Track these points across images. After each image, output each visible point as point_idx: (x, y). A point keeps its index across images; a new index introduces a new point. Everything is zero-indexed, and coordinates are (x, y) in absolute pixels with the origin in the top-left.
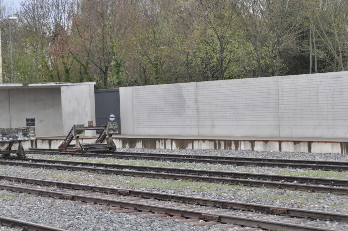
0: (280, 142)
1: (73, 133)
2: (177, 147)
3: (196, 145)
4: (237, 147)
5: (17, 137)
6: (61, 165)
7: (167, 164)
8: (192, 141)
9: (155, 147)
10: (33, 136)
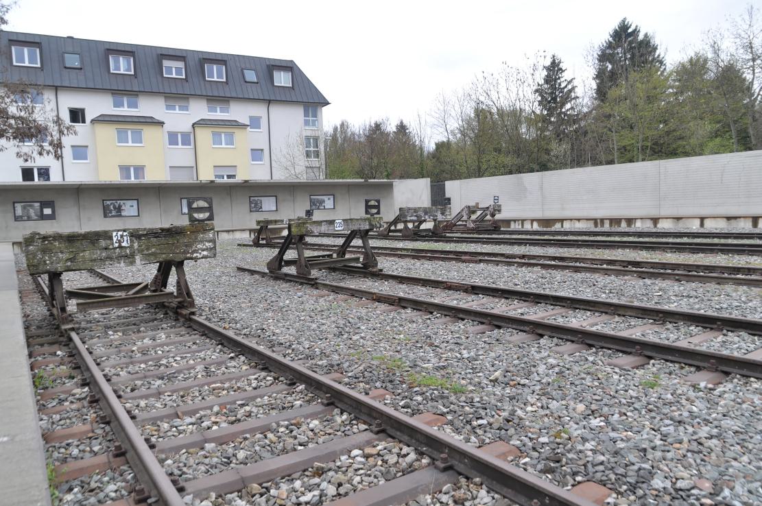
0: (702, 219)
1: (464, 214)
2: (539, 226)
5: (437, 216)
8: (562, 221)
10: (450, 215)
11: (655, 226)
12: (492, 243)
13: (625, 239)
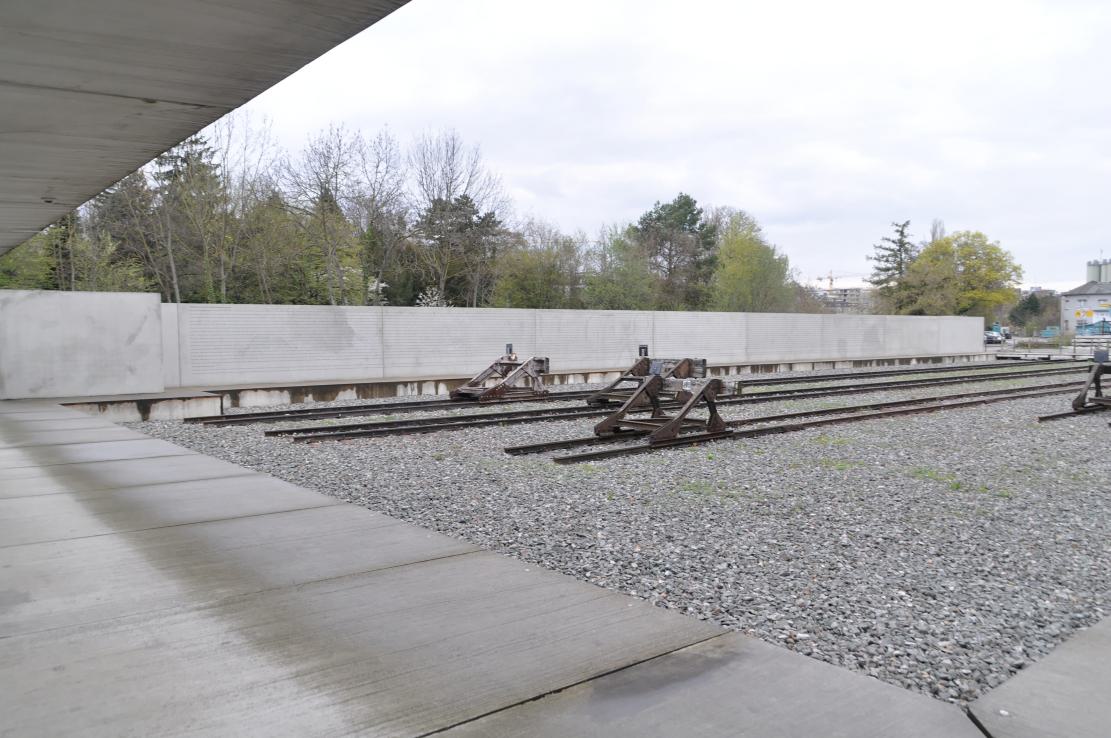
3: (977, 359)
4: (562, 382)
6: (360, 430)
11: (586, 382)
12: (918, 386)
13: (773, 388)
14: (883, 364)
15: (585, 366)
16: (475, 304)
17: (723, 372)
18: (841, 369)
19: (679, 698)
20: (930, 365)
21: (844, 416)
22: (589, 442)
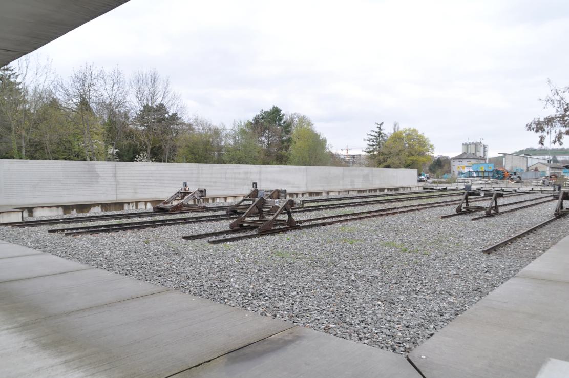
3: (414, 189)
4: (213, 202)
6: (103, 228)
7: (335, 202)
9: (123, 209)
13: (319, 204)
14: (372, 192)
15: (225, 193)
16: (167, 161)
17: (295, 196)
18: (352, 194)
19: (269, 361)
20: (394, 192)
21: (353, 217)
22: (227, 232)
